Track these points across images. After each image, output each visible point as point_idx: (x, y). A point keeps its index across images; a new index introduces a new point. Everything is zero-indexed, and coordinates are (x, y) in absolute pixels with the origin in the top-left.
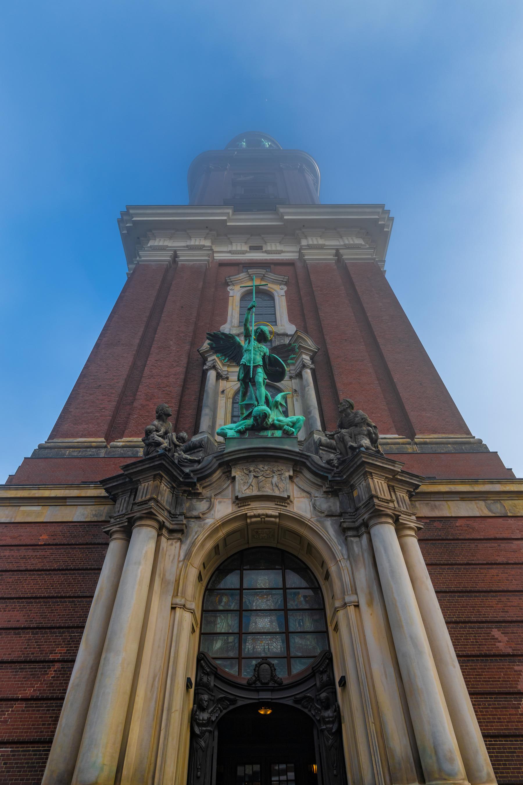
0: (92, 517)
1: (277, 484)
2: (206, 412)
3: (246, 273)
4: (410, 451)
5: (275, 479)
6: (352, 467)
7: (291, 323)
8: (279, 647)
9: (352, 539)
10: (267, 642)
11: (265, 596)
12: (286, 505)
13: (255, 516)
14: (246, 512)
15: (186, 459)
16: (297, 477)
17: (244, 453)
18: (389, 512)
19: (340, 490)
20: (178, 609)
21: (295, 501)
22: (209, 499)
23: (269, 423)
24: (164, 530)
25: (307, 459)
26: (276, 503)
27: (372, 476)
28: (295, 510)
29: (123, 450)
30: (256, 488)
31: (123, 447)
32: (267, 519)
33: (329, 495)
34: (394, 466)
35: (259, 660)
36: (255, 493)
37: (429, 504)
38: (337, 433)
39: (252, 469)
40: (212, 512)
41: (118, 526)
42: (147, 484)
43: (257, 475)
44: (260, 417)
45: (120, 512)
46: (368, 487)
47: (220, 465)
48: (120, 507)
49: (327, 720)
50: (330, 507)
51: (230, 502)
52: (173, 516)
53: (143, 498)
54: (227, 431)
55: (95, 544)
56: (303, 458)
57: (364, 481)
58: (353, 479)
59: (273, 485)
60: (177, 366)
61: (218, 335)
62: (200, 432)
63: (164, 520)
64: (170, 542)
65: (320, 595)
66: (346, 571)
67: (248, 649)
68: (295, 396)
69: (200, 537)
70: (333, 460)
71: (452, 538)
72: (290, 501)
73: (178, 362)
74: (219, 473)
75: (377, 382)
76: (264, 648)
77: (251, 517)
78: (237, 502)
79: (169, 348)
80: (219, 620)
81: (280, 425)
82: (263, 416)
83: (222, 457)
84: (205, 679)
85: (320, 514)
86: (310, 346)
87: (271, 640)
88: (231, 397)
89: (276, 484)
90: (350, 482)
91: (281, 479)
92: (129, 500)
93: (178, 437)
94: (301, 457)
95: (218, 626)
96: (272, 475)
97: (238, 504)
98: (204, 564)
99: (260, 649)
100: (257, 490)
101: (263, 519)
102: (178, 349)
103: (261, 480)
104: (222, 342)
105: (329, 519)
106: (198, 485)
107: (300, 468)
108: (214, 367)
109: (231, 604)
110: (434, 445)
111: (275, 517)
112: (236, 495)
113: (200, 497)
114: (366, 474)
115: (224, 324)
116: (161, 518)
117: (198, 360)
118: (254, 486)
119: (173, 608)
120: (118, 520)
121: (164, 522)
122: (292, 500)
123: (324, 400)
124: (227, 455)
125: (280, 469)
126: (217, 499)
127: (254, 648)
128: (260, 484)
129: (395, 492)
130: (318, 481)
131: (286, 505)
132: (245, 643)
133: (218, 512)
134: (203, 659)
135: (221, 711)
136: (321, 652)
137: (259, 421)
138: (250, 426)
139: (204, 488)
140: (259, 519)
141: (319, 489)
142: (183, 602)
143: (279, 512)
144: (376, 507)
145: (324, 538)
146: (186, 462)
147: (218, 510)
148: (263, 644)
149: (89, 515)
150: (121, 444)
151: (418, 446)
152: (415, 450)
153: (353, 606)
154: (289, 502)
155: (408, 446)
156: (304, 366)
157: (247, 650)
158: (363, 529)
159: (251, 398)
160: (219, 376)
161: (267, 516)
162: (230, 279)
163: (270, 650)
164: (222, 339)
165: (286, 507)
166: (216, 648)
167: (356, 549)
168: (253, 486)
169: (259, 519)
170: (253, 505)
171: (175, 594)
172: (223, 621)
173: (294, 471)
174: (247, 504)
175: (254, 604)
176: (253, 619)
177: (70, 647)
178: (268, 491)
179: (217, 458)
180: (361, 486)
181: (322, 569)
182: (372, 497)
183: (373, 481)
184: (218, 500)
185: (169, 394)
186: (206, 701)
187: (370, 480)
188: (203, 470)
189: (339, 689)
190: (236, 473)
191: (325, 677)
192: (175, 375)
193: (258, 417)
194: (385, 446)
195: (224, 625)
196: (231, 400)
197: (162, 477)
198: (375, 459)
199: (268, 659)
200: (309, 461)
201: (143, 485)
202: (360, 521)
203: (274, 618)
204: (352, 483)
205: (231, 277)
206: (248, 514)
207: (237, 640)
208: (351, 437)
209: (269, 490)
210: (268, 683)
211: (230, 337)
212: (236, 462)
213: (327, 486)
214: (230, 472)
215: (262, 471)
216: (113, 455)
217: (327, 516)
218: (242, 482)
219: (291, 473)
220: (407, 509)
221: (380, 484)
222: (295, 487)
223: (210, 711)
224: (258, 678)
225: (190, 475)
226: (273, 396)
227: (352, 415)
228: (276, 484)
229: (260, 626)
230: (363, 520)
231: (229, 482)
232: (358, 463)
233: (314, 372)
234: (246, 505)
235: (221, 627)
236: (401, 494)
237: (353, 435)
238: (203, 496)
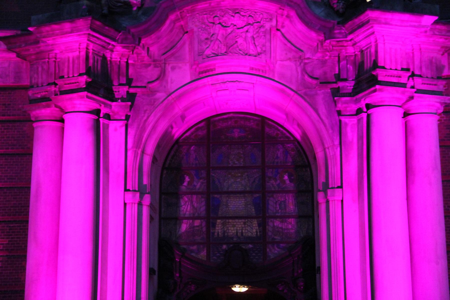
8: (254, 231)
67: (218, 232)
69: (151, 118)
76: (237, 232)
80: (182, 202)
95: (182, 209)
99: (231, 234)
109: (195, 183)
126: (169, 64)
127: (224, 232)
133: (172, 83)
146: (120, 6)
147: (171, 80)
157: (216, 234)
163: (244, 234)
172: (187, 204)
177: (12, 238)
195: (189, 208)
207: (204, 224)
235: (185, 210)
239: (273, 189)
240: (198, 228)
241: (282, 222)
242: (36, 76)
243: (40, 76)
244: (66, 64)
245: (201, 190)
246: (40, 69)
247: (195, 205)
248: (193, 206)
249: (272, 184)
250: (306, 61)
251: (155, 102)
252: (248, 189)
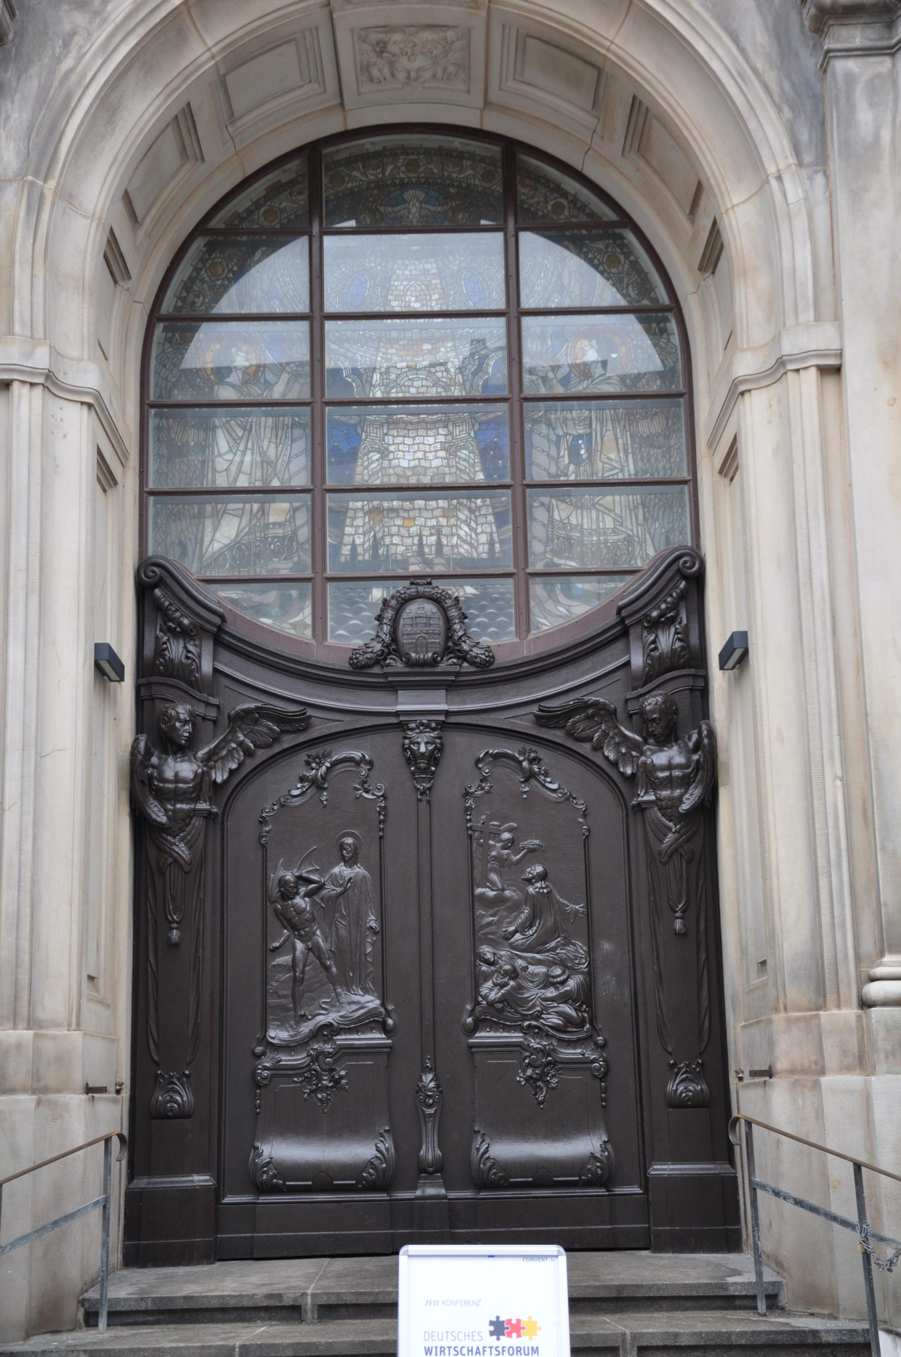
8: (483, 538)
9: (852, 65)
10: (433, 522)
11: (427, 347)
35: (402, 585)
49: (661, 775)
65: (676, 339)
66: (801, 224)
67: (354, 547)
76: (421, 545)
80: (222, 442)
84: (176, 650)
87: (447, 513)
98: (127, 197)
99: (401, 549)
127: (376, 544)
132: (341, 526)
134: (160, 583)
135: (249, 753)
136: (658, 561)
142: (41, 359)
145: (715, 65)
148: (413, 530)
153: (813, 372)
157: (346, 550)
163: (446, 550)
166: (216, 546)
172: (242, 447)
176: (371, 436)
181: (693, 222)
186: (186, 722)
189: (718, 679)
191: (666, 641)
199: (435, 583)
207: (302, 517)
210: (434, 663)
223: (200, 754)
224: (393, 647)
229: (404, 464)
235: (234, 468)
247: (272, 453)
248: (263, 453)
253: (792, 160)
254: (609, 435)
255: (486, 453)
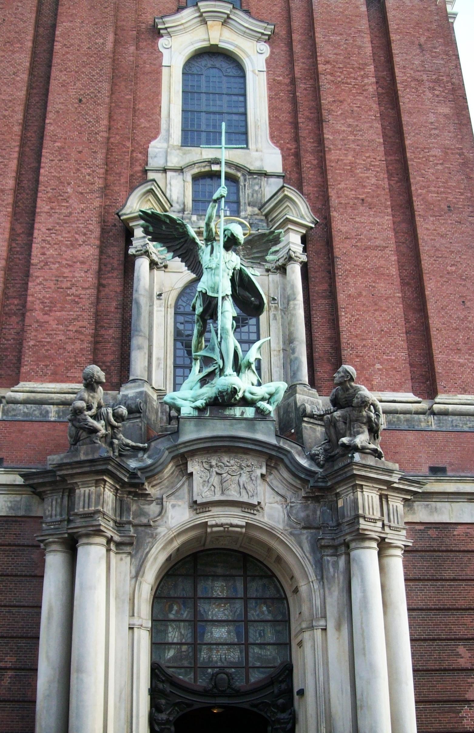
0: (8, 510)
1: (246, 486)
2: (137, 341)
3: (196, 8)
4: (423, 425)
5: (244, 478)
6: (340, 475)
7: (274, 143)
8: (237, 656)
9: (329, 558)
10: (224, 652)
11: (223, 605)
12: (255, 512)
13: (217, 525)
14: (206, 520)
15: (127, 445)
16: (271, 474)
17: (205, 442)
18: (374, 535)
19: (322, 497)
20: (136, 630)
21: (266, 509)
22: (160, 502)
23: (238, 398)
24: (112, 545)
25: (286, 455)
26: (243, 510)
27: (362, 489)
28: (266, 520)
29: (27, 409)
30: (219, 489)
31: (25, 402)
32: (231, 529)
33: (309, 500)
34: (391, 476)
35: (216, 670)
36: (218, 497)
37: (430, 506)
38: (328, 414)
39: (214, 463)
40: (165, 519)
41: (55, 537)
42: (87, 490)
43: (219, 472)
44: (226, 394)
45: (54, 517)
46: (356, 501)
47: (173, 458)
48: (52, 510)
49: (282, 721)
50: (308, 516)
51: (186, 506)
52: (119, 526)
53: (86, 509)
54: (179, 402)
55: (19, 545)
56: (280, 453)
57: (352, 494)
58: (340, 487)
59: (240, 486)
60: (84, 242)
61: (159, 217)
62: (131, 378)
63: (112, 535)
64: (119, 556)
65: (286, 605)
67: (204, 658)
68: (272, 309)
70: (318, 455)
71: (444, 549)
72: (260, 507)
73: (85, 234)
74: (172, 467)
75: (400, 295)
76: (221, 658)
77: (212, 526)
78: (195, 508)
79: (67, 202)
80: (170, 629)
81: (252, 399)
82: (231, 391)
83: (175, 448)
84: (161, 686)
85: (295, 525)
86: (302, 217)
87: (228, 649)
88: (173, 305)
89: (244, 485)
90: (336, 490)
91: (251, 478)
92: (62, 502)
93: (116, 415)
94: (277, 451)
95: (170, 635)
96: (239, 473)
97: (196, 510)
100: (221, 492)
101: (226, 529)
102: (82, 206)
103: (225, 479)
104: (164, 228)
105: (305, 531)
106: (146, 484)
107: (276, 464)
108: (147, 253)
109: (182, 612)
110: (456, 417)
111: (241, 527)
112: (195, 499)
113: (148, 499)
114: (355, 487)
115: (155, 138)
116: (109, 534)
117: (115, 225)
118: (216, 486)
119: (131, 628)
120: (52, 527)
121: (112, 537)
122: (263, 507)
123: (316, 319)
124: (183, 446)
125: (249, 464)
126: (169, 502)
127: (210, 657)
128: (224, 484)
129: (387, 501)
130: (297, 483)
131: (255, 512)
132: (201, 652)
133: (172, 518)
134: (157, 668)
136: (281, 664)
137: (226, 398)
138: (212, 400)
139: (153, 486)
140: (222, 529)
141: (297, 492)
143: (247, 521)
144: (361, 531)
146: (128, 450)
147: (172, 516)
148: (219, 654)
149: (4, 507)
150: (20, 396)
151: (436, 418)
152: (430, 423)
153: (320, 630)
154: (259, 508)
155: (421, 416)
156: (290, 259)
157: (202, 659)
158: (343, 548)
159: (213, 349)
160: (153, 265)
161: (232, 525)
162: (164, 23)
163: (227, 659)
164: (165, 223)
165: (255, 515)
166: (169, 657)
167: (331, 570)
168: (215, 487)
169: (222, 529)
170: (215, 511)
171: (131, 614)
173: (267, 465)
174: (207, 510)
175: (210, 613)
176: (208, 628)
177: (19, 657)
178: (233, 495)
179: (170, 450)
180: (348, 498)
182: (358, 516)
183: (363, 495)
184: (171, 503)
185: (77, 303)
187: (359, 494)
188: (152, 468)
189: (296, 697)
190: (194, 467)
191: (284, 686)
192: (82, 263)
193: (225, 394)
194: (391, 416)
195: (177, 635)
196: (173, 310)
197: (105, 481)
198: (369, 470)
199: (225, 669)
200: (288, 458)
201: (82, 490)
202: (341, 540)
203: (231, 628)
204: (338, 491)
205: (165, 19)
206: (209, 523)
208: (345, 423)
209: (236, 494)
210: (225, 690)
211: (179, 224)
212: (193, 453)
213: (308, 490)
214: (186, 465)
215: (227, 466)
216: (15, 415)
217: (304, 528)
218: (201, 480)
219: (264, 471)
220: (398, 523)
221: (370, 498)
222: (268, 488)
224: (215, 686)
225: (136, 474)
226: (245, 352)
227: (351, 391)
228: (244, 485)
230: (344, 540)
231: (184, 479)
232: (349, 474)
233: (305, 268)
234: (206, 512)
236: (395, 504)
237: (348, 420)
238: (152, 497)
239: (253, 619)
240: (185, 653)
241: (261, 648)
242: (50, 508)
243: (54, 509)
244: (82, 498)
245: (187, 619)
246: (54, 503)
247: (183, 632)
248: (181, 633)
249: (253, 615)
250: (292, 505)
251: (156, 535)
252: (230, 618)
253: (315, 578)
254: (269, 630)
255: (238, 634)
